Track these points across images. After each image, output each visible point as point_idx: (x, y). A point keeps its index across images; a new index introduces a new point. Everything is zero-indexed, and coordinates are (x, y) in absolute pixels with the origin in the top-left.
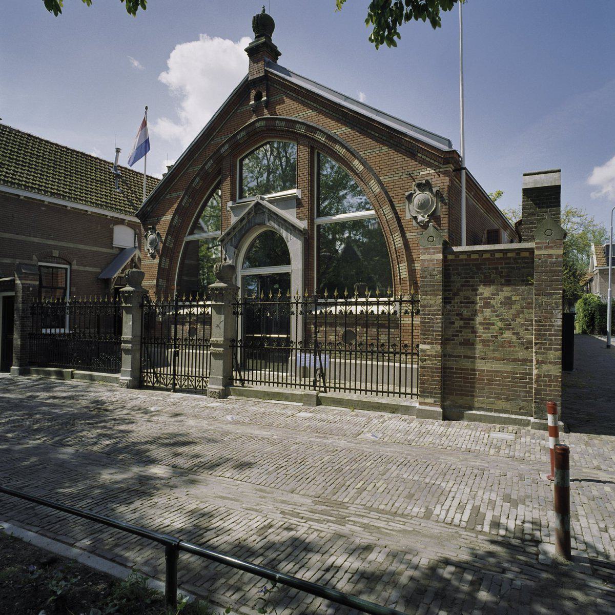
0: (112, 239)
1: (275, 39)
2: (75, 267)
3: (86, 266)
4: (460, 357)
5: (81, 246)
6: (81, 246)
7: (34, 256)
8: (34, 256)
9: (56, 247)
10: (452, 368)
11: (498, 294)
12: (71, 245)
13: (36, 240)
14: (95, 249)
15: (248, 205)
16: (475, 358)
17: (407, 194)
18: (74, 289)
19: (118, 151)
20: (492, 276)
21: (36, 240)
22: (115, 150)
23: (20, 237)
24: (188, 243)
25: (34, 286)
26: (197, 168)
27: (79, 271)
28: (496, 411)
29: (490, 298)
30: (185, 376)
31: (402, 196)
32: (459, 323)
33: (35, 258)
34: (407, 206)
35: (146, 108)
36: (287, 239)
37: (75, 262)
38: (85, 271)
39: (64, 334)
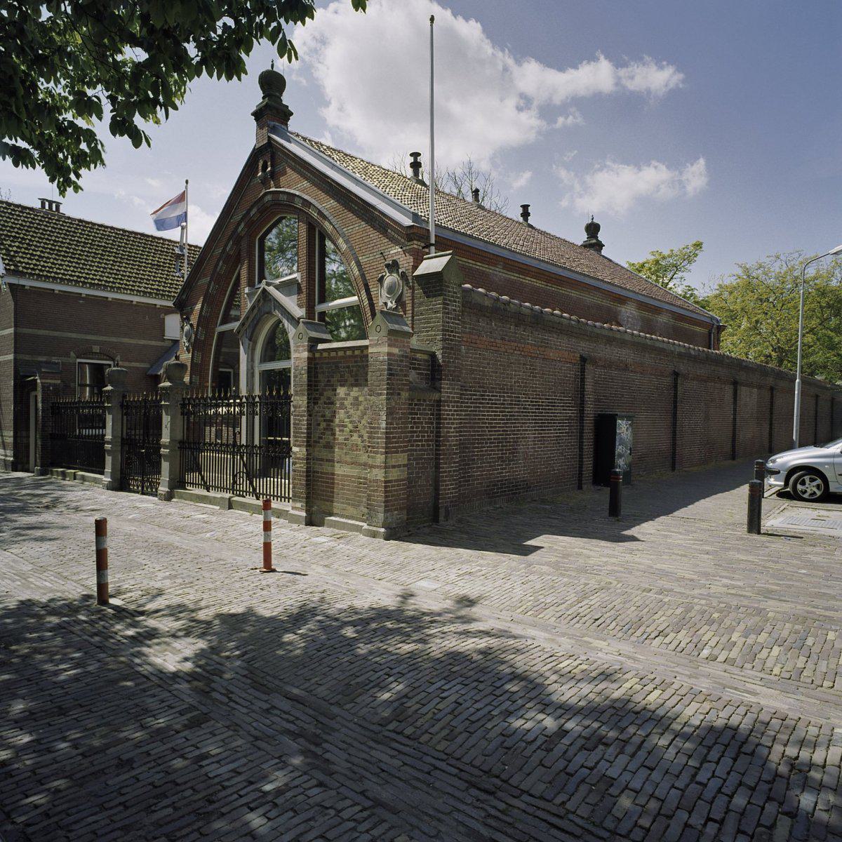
1: (287, 99)
4: (322, 460)
5: (126, 340)
6: (126, 340)
9: (96, 343)
10: (318, 472)
11: (349, 395)
12: (114, 339)
13: (74, 335)
14: (142, 342)
16: (333, 461)
17: (380, 275)
20: (347, 374)
21: (74, 335)
23: (56, 334)
24: (222, 334)
25: (54, 385)
28: (347, 517)
29: (344, 399)
32: (323, 425)
33: (72, 354)
35: (187, 182)
37: (118, 358)
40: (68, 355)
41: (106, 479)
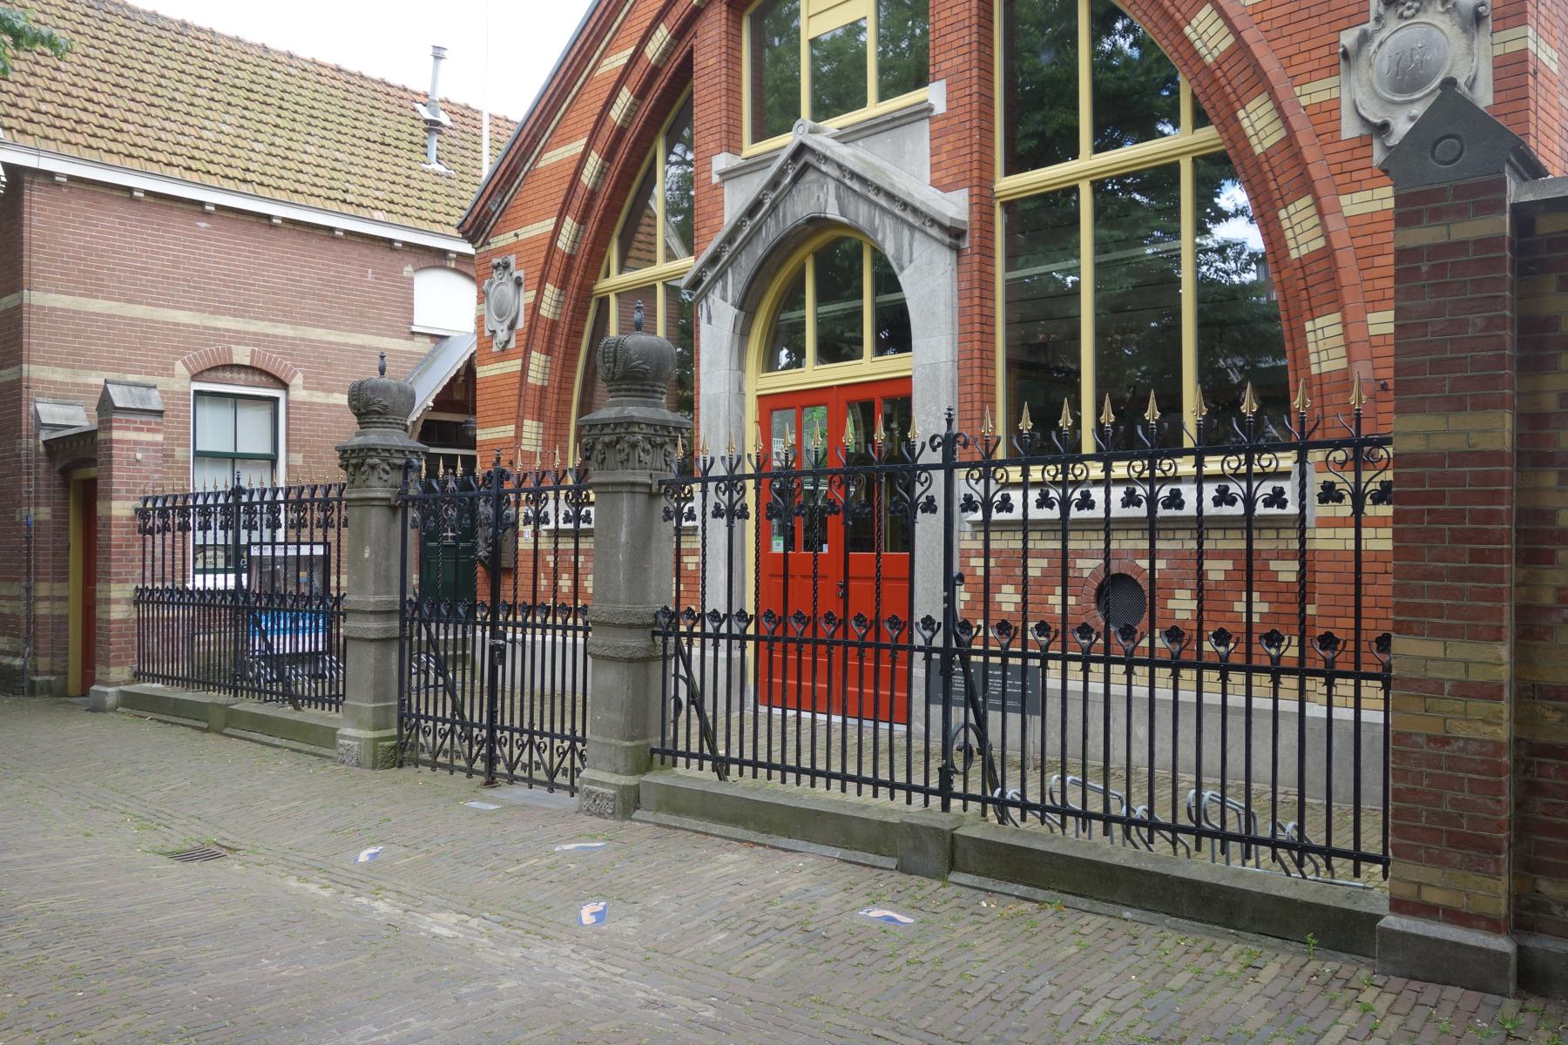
0: (411, 311)
3: (332, 391)
9: (240, 338)
13: (183, 317)
15: (775, 158)
18: (298, 459)
19: (438, 54)
21: (183, 317)
22: (431, 50)
26: (619, 59)
30: (522, 732)
31: (1325, 51)
33: (180, 368)
34: (1345, 90)
36: (899, 259)
37: (297, 381)
38: (328, 405)
40: (167, 371)
41: (354, 733)
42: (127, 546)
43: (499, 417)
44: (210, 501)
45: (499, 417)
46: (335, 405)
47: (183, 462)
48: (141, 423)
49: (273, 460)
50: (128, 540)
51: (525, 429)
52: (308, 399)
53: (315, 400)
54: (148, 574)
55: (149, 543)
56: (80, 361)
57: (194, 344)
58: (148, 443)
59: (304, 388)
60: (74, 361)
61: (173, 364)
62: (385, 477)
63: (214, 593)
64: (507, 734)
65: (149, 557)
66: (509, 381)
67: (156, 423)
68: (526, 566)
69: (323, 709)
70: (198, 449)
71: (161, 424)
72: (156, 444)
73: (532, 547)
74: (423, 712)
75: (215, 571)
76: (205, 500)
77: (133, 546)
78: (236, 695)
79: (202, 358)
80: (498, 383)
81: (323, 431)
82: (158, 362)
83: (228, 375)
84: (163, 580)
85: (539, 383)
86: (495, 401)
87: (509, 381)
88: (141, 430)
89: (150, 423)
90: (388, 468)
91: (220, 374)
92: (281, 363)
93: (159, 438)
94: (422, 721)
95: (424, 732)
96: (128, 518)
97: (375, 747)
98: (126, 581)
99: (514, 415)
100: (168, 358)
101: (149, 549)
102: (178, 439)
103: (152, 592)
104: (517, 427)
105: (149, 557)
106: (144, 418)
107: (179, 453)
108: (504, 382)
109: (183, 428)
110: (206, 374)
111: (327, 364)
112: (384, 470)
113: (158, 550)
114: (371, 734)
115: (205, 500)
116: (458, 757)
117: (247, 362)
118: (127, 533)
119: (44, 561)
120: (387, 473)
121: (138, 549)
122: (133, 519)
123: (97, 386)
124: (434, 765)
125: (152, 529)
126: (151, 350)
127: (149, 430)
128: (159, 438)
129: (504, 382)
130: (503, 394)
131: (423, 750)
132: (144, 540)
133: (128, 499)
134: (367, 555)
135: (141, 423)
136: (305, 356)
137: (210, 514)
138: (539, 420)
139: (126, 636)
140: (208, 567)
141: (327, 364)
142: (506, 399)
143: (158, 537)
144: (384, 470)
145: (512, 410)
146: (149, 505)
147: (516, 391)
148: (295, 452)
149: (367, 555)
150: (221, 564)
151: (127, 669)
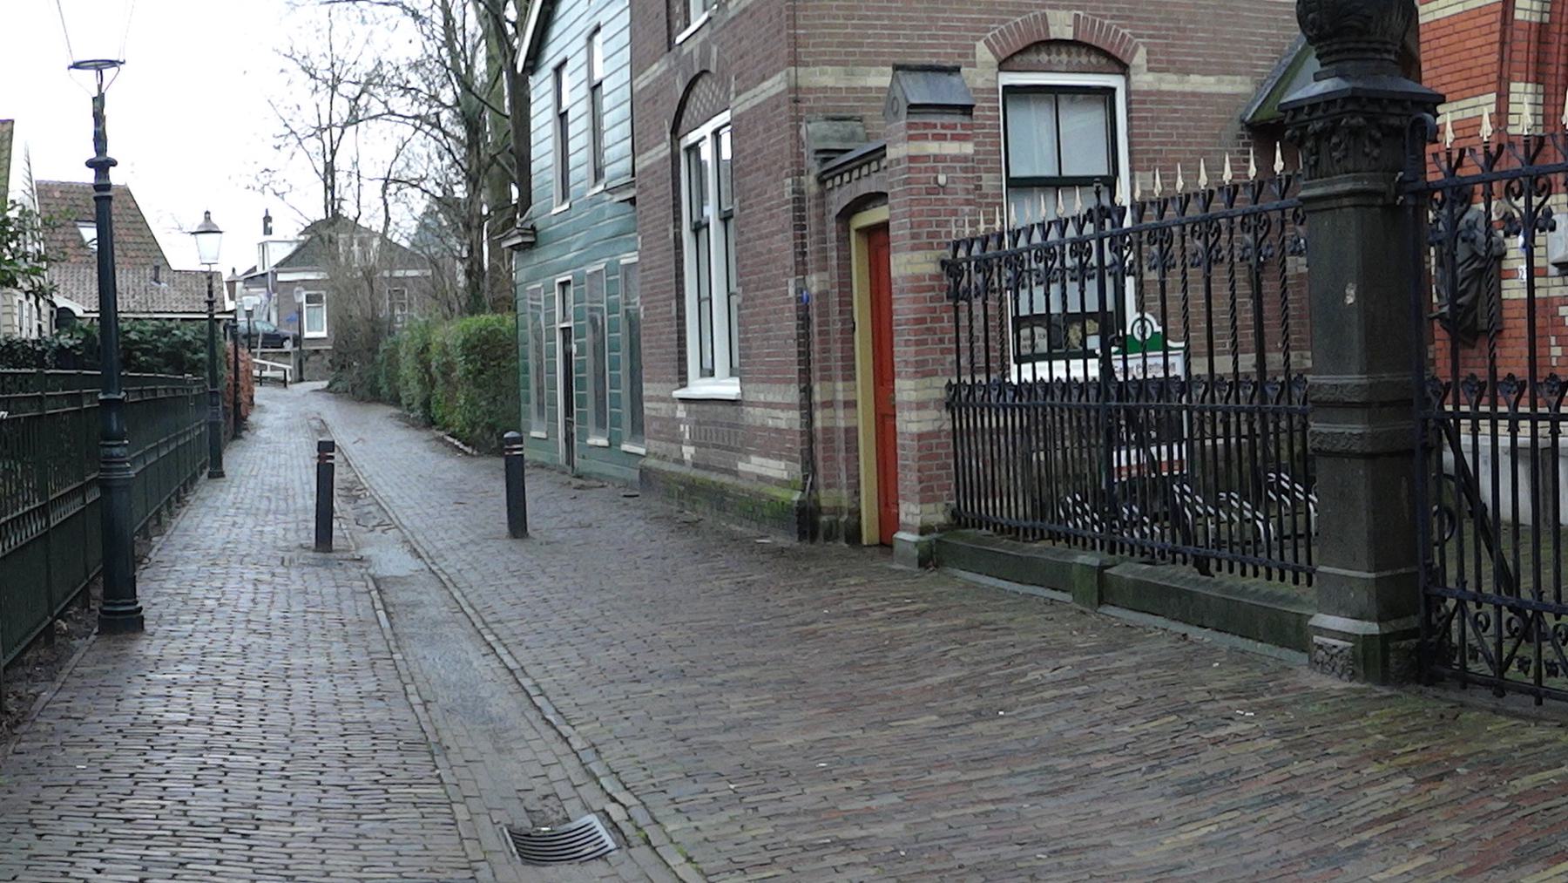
2: (1144, 80)
7: (981, 46)
8: (981, 46)
27: (1160, 97)
33: (983, 53)
37: (1140, 59)
38: (1184, 94)
39: (1165, 384)
42: (933, 320)
43: (1463, 84)
44: (1053, 235)
45: (1463, 84)
46: (1194, 94)
47: (994, 196)
48: (943, 127)
49: (1110, 182)
50: (934, 310)
51: (1513, 98)
52: (1155, 87)
53: (1165, 87)
54: (964, 361)
55: (964, 316)
56: (854, 54)
57: (1001, 13)
58: (955, 158)
59: (1150, 70)
60: (847, 54)
61: (974, 46)
62: (1376, 152)
63: (1068, 385)
64: (1488, 608)
65: (964, 335)
66: (1483, 20)
67: (963, 126)
68: (1516, 324)
69: (1269, 577)
70: (1012, 175)
71: (972, 127)
72: (965, 158)
73: (1525, 295)
74: (1471, 588)
75: (1033, 358)
76: (1045, 235)
77: (942, 320)
78: (1112, 552)
79: (1012, 34)
80: (1459, 27)
81: (1179, 135)
82: (954, 46)
83: (1044, 57)
84: (988, 371)
85: (1535, 18)
86: (1455, 57)
87: (1483, 20)
88: (942, 138)
89: (954, 127)
90: (1379, 135)
91: (1033, 58)
92: (1117, 32)
93: (968, 148)
94: (1471, 606)
95: (1476, 623)
96: (932, 277)
97: (1385, 650)
98: (933, 373)
99: (1494, 77)
100: (966, 38)
101: (964, 322)
102: (984, 161)
103: (972, 388)
104: (1499, 96)
105: (964, 335)
106: (947, 119)
107: (988, 181)
108: (1470, 24)
109: (992, 144)
110: (1017, 59)
111: (1178, 29)
112: (1371, 138)
113: (979, 324)
114: (1373, 628)
115: (1045, 235)
116: (1475, 658)
117: (1068, 35)
118: (932, 300)
119: (974, 224)
120: (1377, 144)
121: (948, 324)
122: (937, 277)
123: (880, 89)
124: (1499, 687)
125: (967, 290)
126: (943, 28)
127: (955, 138)
128: (968, 148)
129: (1470, 24)
130: (1469, 44)
131: (1475, 658)
132: (957, 309)
133: (930, 247)
134: (1350, 300)
135: (943, 127)
136: (1148, 19)
137: (1054, 257)
138: (1537, 82)
139: (938, 456)
140: (1023, 352)
141: (1178, 29)
142: (1477, 52)
143: (977, 303)
144: (1371, 138)
145: (1487, 69)
146: (962, 253)
147: (1497, 37)
148: (1141, 169)
149: (1350, 300)
150: (1042, 345)
151: (941, 506)
